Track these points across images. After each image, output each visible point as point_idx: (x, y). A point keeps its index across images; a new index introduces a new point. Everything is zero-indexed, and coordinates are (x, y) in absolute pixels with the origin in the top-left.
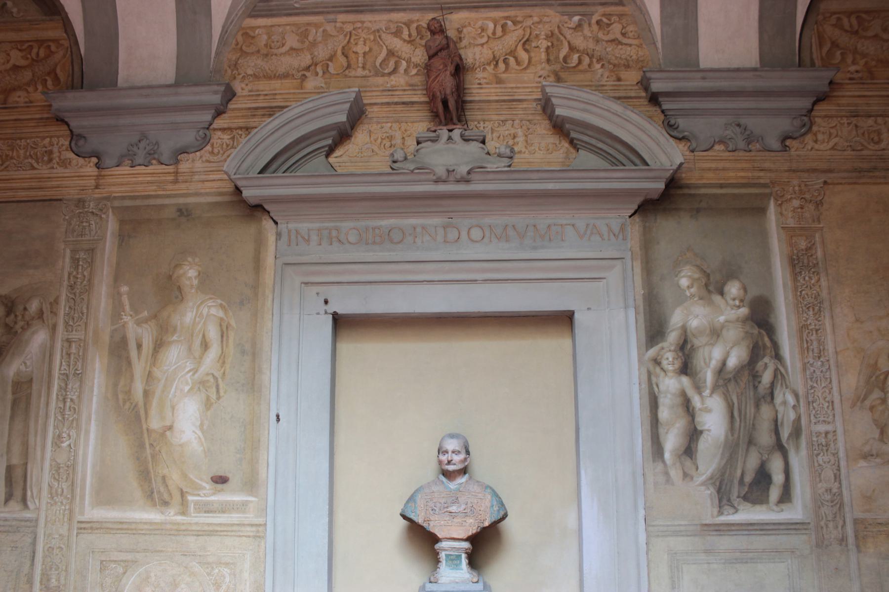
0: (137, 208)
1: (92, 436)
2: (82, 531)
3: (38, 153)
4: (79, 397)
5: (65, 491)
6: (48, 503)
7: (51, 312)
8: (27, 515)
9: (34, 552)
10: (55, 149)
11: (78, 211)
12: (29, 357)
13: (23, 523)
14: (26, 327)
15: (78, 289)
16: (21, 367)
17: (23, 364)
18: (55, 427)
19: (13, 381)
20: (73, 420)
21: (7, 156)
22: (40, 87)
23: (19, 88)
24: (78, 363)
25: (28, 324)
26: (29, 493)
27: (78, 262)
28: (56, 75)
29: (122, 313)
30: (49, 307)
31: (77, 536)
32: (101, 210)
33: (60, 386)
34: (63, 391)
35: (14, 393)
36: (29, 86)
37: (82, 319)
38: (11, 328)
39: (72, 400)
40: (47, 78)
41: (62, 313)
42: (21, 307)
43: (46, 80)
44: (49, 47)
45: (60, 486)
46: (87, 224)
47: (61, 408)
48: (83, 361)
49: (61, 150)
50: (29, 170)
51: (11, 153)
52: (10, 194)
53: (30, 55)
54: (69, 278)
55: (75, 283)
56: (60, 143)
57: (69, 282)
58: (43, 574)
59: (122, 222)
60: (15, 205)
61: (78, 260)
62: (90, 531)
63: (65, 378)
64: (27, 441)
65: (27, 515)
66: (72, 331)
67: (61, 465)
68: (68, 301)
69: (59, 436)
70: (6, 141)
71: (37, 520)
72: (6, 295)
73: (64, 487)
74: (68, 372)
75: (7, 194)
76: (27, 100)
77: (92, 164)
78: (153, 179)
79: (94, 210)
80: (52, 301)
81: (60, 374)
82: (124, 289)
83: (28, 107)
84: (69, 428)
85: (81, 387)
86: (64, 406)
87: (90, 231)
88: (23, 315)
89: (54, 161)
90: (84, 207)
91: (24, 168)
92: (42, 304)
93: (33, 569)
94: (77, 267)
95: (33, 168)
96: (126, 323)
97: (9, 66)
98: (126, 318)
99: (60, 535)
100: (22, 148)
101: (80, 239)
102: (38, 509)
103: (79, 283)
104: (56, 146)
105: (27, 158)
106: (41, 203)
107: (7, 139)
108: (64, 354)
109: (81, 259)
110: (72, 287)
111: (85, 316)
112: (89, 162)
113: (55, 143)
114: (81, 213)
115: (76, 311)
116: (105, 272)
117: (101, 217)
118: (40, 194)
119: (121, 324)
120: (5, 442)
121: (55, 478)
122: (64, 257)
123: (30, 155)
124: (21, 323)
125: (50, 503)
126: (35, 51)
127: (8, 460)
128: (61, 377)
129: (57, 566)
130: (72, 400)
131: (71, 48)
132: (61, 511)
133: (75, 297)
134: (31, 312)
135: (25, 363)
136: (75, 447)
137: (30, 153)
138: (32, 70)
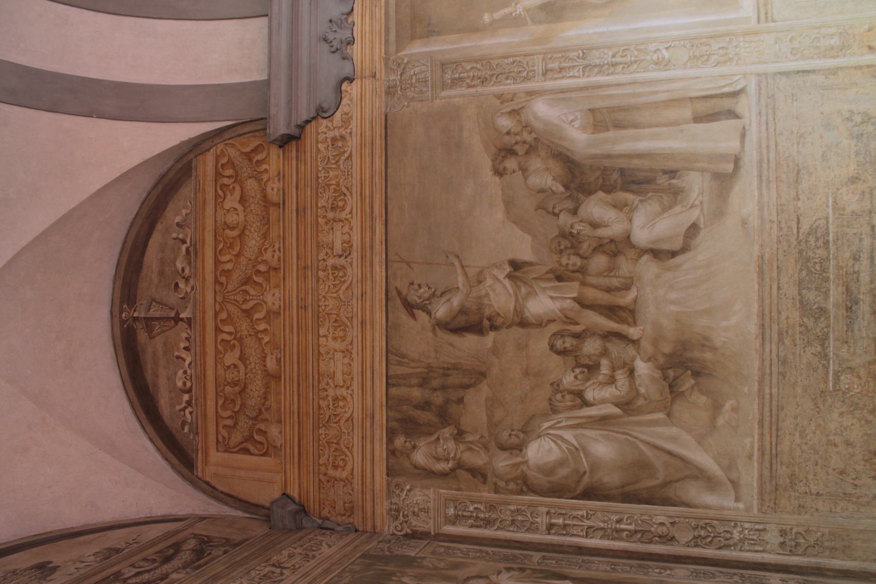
0: (399, 23)
1: (656, 23)
2: (769, 15)
3: (334, 154)
4: (609, 48)
5: (721, 45)
6: (737, 64)
7: (512, 100)
8: (752, 89)
9: (798, 72)
10: (330, 134)
11: (399, 92)
12: (564, 118)
13: (763, 91)
14: (529, 128)
15: (486, 73)
16: (576, 126)
17: (573, 124)
18: (646, 70)
19: (593, 133)
20: (638, 50)
21: (335, 191)
22: (265, 166)
23: (263, 191)
24: (571, 56)
25: (526, 127)
26: (726, 90)
27: (456, 79)
28: (252, 151)
29: (514, 15)
30: (506, 104)
31: (776, 21)
32: (399, 65)
33: (597, 73)
34: (603, 69)
35: (607, 130)
36: (262, 179)
37: (519, 61)
38: (530, 146)
39: (614, 56)
40: (254, 161)
41: (513, 87)
42: (507, 139)
43: (258, 161)
44: (223, 165)
45: (716, 52)
46: (414, 77)
47: (624, 67)
48: (568, 51)
49: (332, 128)
50: (352, 161)
51: (333, 187)
52: (377, 179)
53: (229, 186)
54: (474, 86)
55: (479, 78)
56: (325, 130)
57: (478, 85)
58: (825, 57)
59: (413, 38)
60: (389, 170)
61: (453, 80)
62: (769, 6)
63: (588, 68)
64: (663, 102)
65: (752, 89)
66: (534, 71)
67: (691, 54)
68: (500, 82)
69: (656, 64)
70: (320, 195)
71: (759, 75)
72: (493, 161)
73: (717, 47)
74: (581, 67)
75: (377, 181)
76: (276, 179)
77: (349, 89)
78: (368, 14)
79: (399, 73)
80: (498, 102)
81: (583, 75)
82: (487, 18)
83: (284, 176)
84: (646, 53)
85: (597, 48)
86: (621, 64)
87: (421, 72)
88: (515, 135)
89: (344, 133)
90: (395, 86)
91: (350, 167)
92: (502, 113)
93: (820, 70)
94: (461, 79)
95: (350, 156)
96: (524, 9)
97: (240, 208)
98: (520, 9)
99: (776, 43)
100: (327, 175)
101: (430, 83)
102: (745, 75)
103: (480, 73)
104: (327, 135)
105: (339, 166)
106: (388, 138)
107: (317, 194)
108: (560, 76)
109: (453, 76)
110: (484, 81)
111: (517, 58)
112: (346, 91)
113: (324, 136)
114: (401, 88)
115: (512, 70)
116: (468, 45)
117: (408, 62)
118: (379, 142)
119: (526, 14)
120: (665, 129)
121: (707, 60)
122: (450, 97)
123: (336, 163)
124: (526, 136)
125: (737, 61)
126: (226, 181)
127: (687, 123)
128: (587, 74)
129: (813, 40)
130: (614, 56)
131: (225, 140)
132: (747, 46)
133: (495, 74)
134: (512, 125)
135: (572, 121)
136: (669, 42)
137: (333, 164)
138: (246, 180)
